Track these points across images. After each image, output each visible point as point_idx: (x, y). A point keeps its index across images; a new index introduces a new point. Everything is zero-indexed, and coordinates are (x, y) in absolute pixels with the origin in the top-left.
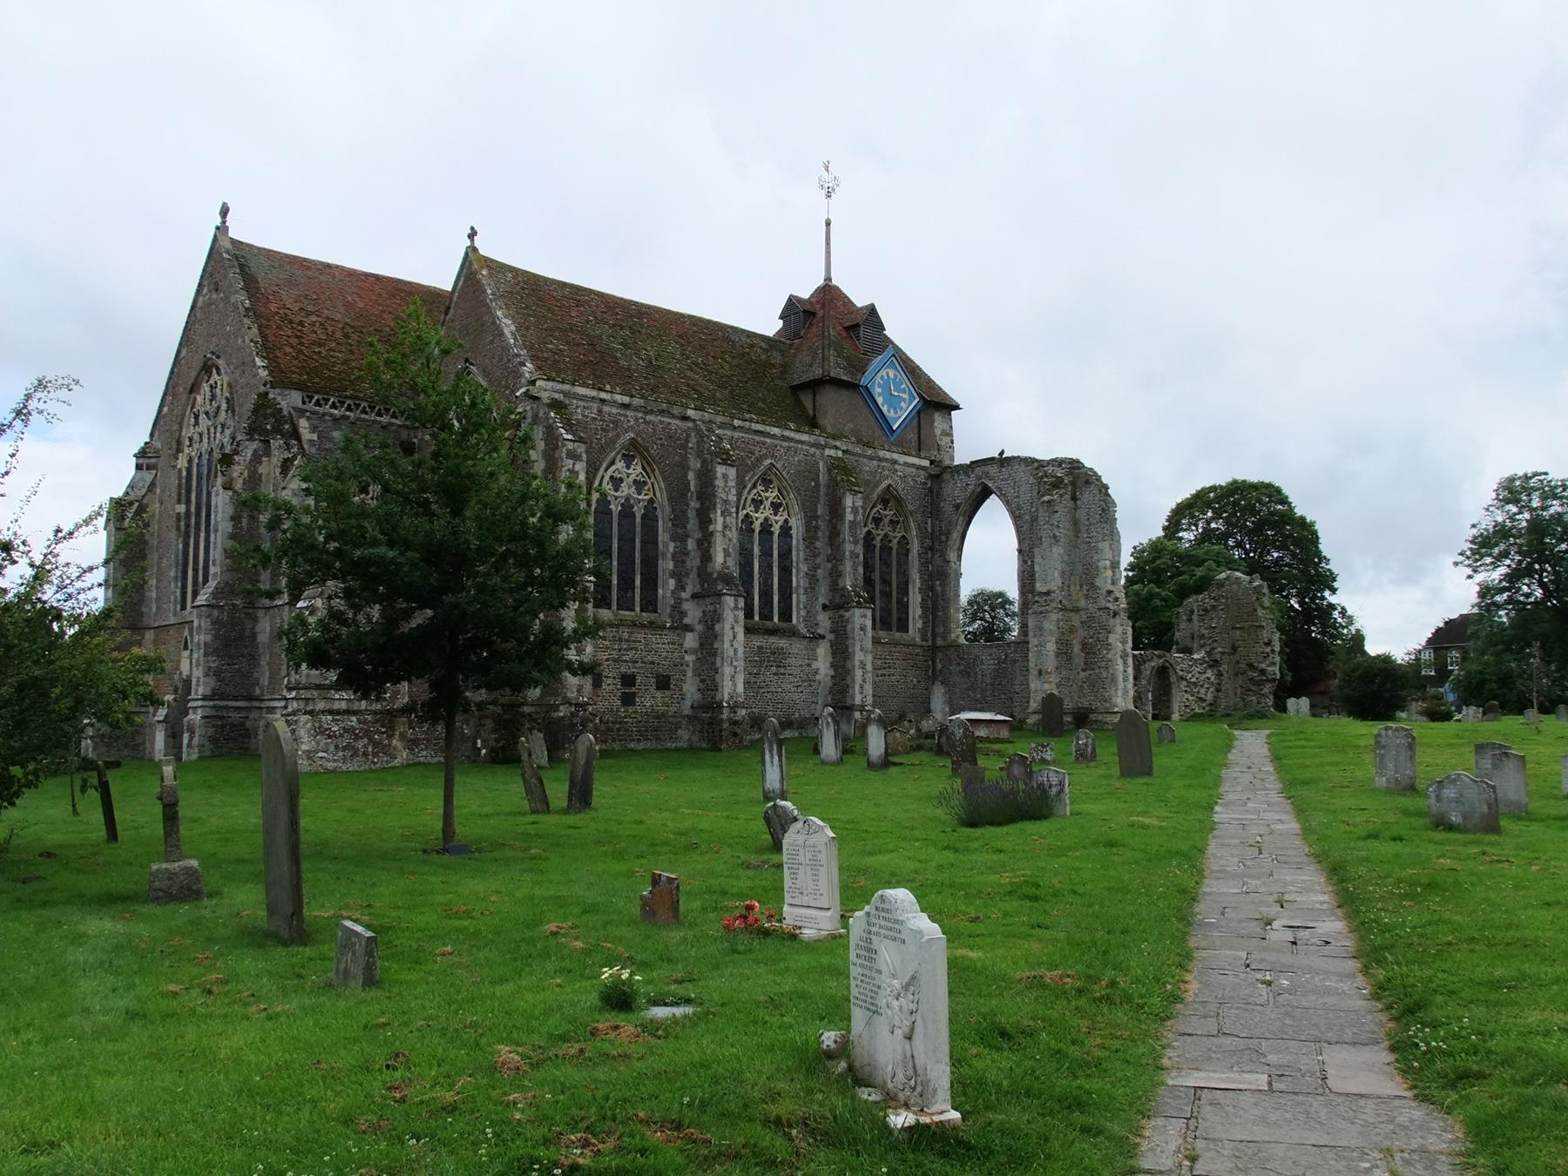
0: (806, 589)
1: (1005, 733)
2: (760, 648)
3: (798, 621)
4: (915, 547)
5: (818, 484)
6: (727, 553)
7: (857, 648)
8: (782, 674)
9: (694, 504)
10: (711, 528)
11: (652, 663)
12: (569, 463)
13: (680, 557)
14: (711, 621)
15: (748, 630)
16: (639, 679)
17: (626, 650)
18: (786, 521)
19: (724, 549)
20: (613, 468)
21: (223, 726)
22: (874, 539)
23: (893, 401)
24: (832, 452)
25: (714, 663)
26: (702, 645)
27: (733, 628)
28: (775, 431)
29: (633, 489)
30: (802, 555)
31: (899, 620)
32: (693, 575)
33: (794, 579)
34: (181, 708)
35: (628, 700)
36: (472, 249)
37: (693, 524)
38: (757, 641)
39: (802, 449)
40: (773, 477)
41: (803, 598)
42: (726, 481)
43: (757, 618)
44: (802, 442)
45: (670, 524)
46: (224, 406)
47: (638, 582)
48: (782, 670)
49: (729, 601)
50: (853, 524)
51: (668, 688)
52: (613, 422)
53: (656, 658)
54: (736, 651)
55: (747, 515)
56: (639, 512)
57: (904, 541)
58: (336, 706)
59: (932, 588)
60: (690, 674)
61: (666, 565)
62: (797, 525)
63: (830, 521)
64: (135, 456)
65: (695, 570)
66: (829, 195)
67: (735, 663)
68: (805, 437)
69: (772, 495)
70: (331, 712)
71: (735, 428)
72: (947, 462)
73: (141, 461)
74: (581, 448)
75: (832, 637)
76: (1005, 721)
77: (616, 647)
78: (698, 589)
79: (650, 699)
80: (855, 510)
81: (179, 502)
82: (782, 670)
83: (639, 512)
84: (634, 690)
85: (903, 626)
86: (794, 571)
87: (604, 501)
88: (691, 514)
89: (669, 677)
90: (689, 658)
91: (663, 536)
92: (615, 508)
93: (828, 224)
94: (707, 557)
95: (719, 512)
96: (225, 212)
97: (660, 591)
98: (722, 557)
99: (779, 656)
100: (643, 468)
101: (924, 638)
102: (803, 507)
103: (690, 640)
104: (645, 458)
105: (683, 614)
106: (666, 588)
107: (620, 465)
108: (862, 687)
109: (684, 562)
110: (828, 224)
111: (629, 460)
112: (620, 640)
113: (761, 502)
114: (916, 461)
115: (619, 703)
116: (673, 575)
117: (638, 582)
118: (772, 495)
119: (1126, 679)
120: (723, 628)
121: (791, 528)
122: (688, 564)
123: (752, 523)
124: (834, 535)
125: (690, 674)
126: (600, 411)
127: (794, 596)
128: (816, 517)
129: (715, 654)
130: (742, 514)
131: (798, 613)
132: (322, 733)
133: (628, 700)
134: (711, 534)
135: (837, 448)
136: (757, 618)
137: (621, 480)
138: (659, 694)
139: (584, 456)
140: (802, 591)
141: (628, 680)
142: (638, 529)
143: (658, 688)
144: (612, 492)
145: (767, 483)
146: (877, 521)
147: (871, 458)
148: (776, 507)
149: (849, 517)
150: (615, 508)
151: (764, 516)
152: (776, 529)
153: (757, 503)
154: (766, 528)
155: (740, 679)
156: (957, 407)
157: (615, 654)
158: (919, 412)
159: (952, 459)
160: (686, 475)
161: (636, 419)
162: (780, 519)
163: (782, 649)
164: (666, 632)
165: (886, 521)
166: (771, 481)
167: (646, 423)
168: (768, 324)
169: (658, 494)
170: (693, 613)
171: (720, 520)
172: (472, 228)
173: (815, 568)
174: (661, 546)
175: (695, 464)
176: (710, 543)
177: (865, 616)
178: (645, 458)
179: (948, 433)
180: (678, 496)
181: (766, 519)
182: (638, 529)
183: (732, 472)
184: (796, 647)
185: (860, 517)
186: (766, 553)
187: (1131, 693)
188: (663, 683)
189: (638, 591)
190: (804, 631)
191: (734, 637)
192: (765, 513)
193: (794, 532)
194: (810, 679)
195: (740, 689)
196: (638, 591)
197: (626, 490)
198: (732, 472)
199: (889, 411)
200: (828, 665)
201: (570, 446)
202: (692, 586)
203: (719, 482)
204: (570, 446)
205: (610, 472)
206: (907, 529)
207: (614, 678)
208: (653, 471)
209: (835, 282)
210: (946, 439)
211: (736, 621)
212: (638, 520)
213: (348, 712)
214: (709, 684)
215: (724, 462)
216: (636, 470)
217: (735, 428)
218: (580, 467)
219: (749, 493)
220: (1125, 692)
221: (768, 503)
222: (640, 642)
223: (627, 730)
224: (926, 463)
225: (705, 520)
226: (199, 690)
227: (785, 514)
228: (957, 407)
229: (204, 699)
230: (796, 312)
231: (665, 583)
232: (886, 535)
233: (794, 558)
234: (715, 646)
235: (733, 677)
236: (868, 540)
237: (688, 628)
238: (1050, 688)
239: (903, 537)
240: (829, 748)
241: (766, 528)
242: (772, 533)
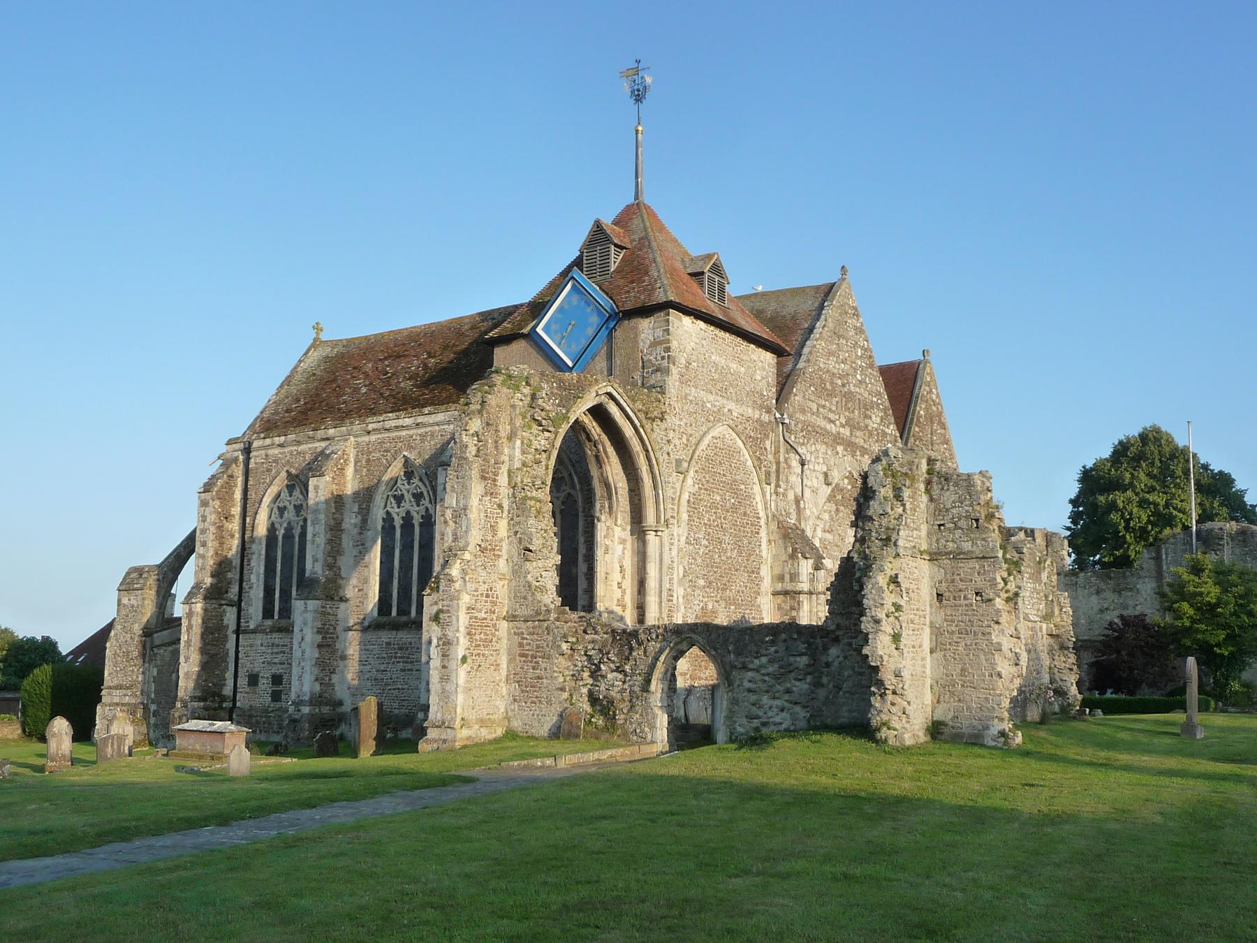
2: (388, 644)
6: (315, 560)
8: (409, 670)
17: (277, 653)
27: (302, 630)
28: (408, 421)
43: (394, 613)
48: (409, 666)
54: (303, 652)
67: (302, 664)
68: (440, 417)
71: (369, 433)
77: (269, 651)
82: (409, 666)
92: (281, 533)
136: (394, 613)
137: (285, 508)
144: (279, 520)
163: (411, 643)
207: (268, 678)
211: (305, 624)
213: (117, 704)
217: (369, 433)
222: (286, 645)
223: (270, 724)
241: (408, 519)
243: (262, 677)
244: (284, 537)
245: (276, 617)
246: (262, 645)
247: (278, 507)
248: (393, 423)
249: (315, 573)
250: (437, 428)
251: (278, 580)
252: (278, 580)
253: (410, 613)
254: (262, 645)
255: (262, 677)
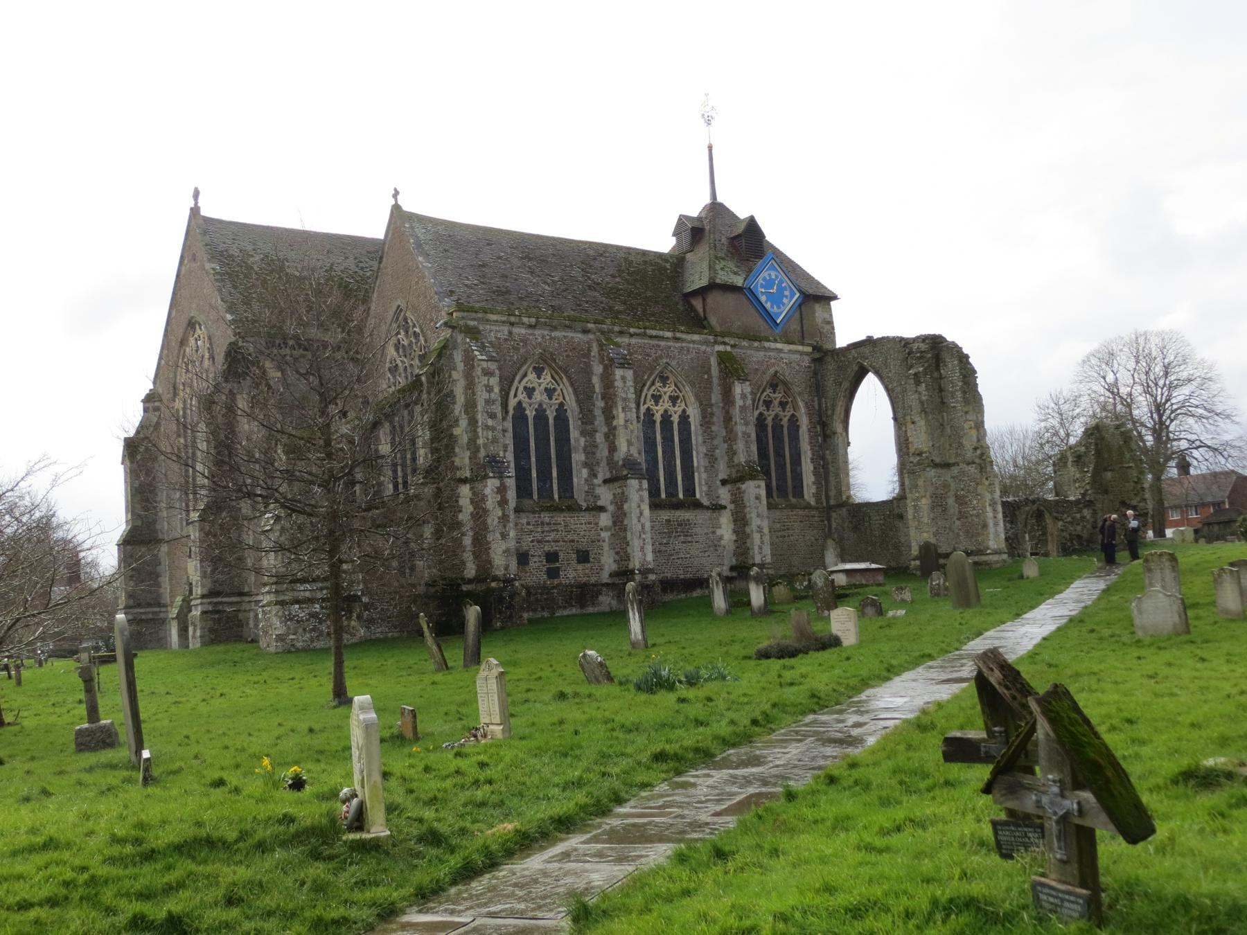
0: (706, 467)
1: (881, 578)
2: (668, 521)
3: (701, 495)
4: (804, 422)
5: (710, 376)
6: (630, 443)
7: (754, 515)
9: (600, 404)
10: (615, 423)
11: (573, 541)
12: (484, 380)
13: (590, 450)
14: (620, 501)
15: (656, 505)
16: (561, 555)
17: (548, 531)
18: (684, 411)
19: (628, 441)
20: (526, 379)
21: (219, 619)
22: (765, 419)
23: (777, 299)
24: (721, 348)
25: (625, 538)
26: (615, 523)
27: (639, 506)
28: (669, 334)
29: (545, 396)
30: (700, 439)
31: (794, 487)
32: (604, 463)
33: (695, 460)
34: (186, 607)
35: (553, 573)
36: (396, 208)
37: (600, 420)
38: (665, 515)
39: (694, 348)
40: (669, 374)
41: (704, 476)
42: (625, 382)
44: (694, 342)
45: (580, 422)
46: (207, 355)
47: (555, 474)
48: (690, 539)
49: (633, 483)
50: (743, 408)
51: (588, 561)
52: (521, 340)
53: (576, 538)
54: (643, 526)
55: (648, 409)
56: (551, 415)
57: (794, 421)
58: (302, 595)
59: (823, 458)
60: (606, 546)
61: (578, 457)
62: (694, 413)
63: (723, 408)
64: (143, 401)
65: (605, 460)
66: (709, 123)
67: (643, 536)
68: (696, 337)
69: (669, 390)
70: (297, 601)
72: (828, 346)
73: (147, 405)
74: (493, 366)
75: (732, 506)
76: (879, 569)
77: (539, 530)
78: (608, 476)
79: (572, 573)
80: (744, 396)
81: (179, 436)
82: (690, 539)
83: (551, 415)
84: (557, 564)
85: (798, 490)
86: (694, 453)
87: (519, 407)
88: (598, 412)
89: (587, 552)
90: (605, 535)
91: (574, 434)
92: (531, 414)
93: (710, 148)
94: (613, 449)
95: (620, 410)
96: (196, 194)
97: (575, 480)
98: (628, 444)
99: (684, 528)
100: (553, 377)
101: (818, 500)
102: (697, 397)
103: (605, 520)
104: (553, 369)
105: (597, 497)
106: (580, 476)
107: (532, 376)
108: (760, 548)
109: (594, 453)
110: (710, 148)
111: (539, 372)
112: (543, 523)
113: (660, 396)
114: (800, 348)
115: (545, 576)
116: (586, 465)
117: (555, 474)
118: (669, 390)
119: (996, 524)
120: (630, 507)
121: (688, 416)
122: (598, 455)
123: (653, 415)
124: (728, 419)
125: (606, 546)
126: (510, 333)
127: (696, 474)
128: (711, 405)
129: (625, 530)
130: (643, 409)
131: (700, 488)
132: (291, 619)
133: (553, 573)
134: (615, 428)
135: (725, 343)
137: (534, 389)
138: (580, 567)
139: (497, 372)
140: (703, 470)
141: (552, 557)
142: (552, 429)
143: (579, 562)
144: (527, 400)
145: (664, 380)
146: (768, 404)
147: (757, 349)
148: (674, 400)
149: (739, 402)
150: (531, 414)
151: (663, 408)
152: (675, 419)
153: (657, 398)
154: (666, 418)
155: (649, 549)
156: (835, 298)
157: (538, 536)
158: (800, 306)
159: (834, 342)
160: (590, 380)
161: (543, 337)
162: (679, 409)
163: (688, 520)
164: (583, 514)
165: (776, 402)
166: (667, 378)
167: (551, 338)
168: (662, 242)
169: (567, 399)
170: (605, 496)
171: (622, 415)
172: (395, 190)
173: (713, 449)
174: (572, 441)
175: (598, 369)
176: (614, 435)
177: (759, 487)
178: (553, 369)
179: (830, 323)
180: (584, 399)
181: (666, 411)
182: (552, 429)
183: (629, 374)
184: (698, 518)
185: (749, 402)
186: (668, 439)
187: (1003, 536)
188: (583, 557)
189: (555, 482)
190: (706, 502)
191: (641, 514)
192: (665, 404)
193: (691, 419)
194: (716, 545)
195: (650, 557)
196: (555, 482)
197: (539, 396)
198: (629, 374)
199: (772, 307)
200: (730, 531)
201: (484, 364)
202: (603, 472)
203: (618, 383)
204: (484, 364)
205: (523, 383)
206: (795, 408)
207: (540, 556)
208: (561, 379)
209: (720, 199)
210: (828, 327)
211: (642, 500)
212: (551, 421)
214: (623, 555)
215: (622, 366)
216: (547, 379)
217: (631, 336)
218: (494, 381)
219: (648, 390)
220: (997, 534)
221: (666, 398)
224: (809, 349)
225: (609, 416)
226: (198, 591)
227: (683, 406)
228: (835, 298)
229: (203, 597)
230: (677, 233)
231: (579, 472)
232: (776, 416)
233: (694, 442)
234: (625, 523)
235: (642, 549)
236: (761, 423)
237: (602, 509)
238: (927, 536)
239: (793, 415)
240: (720, 600)
241: (666, 418)
242: (672, 423)
243: (532, 556)
244: (535, 418)
245: (535, 497)
246: (528, 524)
247: (525, 388)
248: (654, 333)
249: (631, 455)
250: (691, 345)
251: (533, 459)
252: (533, 459)
253: (677, 495)
254: (528, 524)
255: (532, 556)
